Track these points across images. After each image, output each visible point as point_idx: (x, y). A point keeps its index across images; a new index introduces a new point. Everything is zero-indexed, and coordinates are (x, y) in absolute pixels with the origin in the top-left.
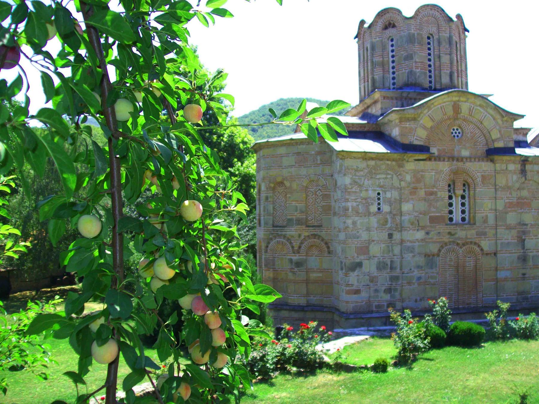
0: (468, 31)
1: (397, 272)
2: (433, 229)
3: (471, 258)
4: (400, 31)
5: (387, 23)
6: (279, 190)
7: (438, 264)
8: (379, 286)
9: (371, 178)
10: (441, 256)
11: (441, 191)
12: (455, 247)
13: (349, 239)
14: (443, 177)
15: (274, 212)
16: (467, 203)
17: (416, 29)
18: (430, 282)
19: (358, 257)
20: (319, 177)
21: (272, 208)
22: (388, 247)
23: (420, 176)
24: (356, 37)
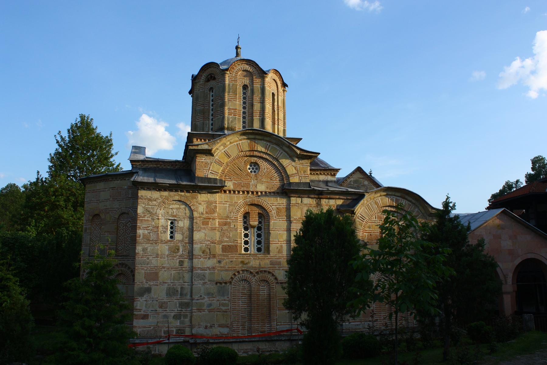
0: (287, 86)
1: (187, 299)
2: (225, 258)
3: (265, 287)
4: (219, 82)
5: (209, 77)
6: (96, 222)
7: (230, 291)
8: (168, 311)
9: (165, 207)
10: (233, 284)
11: (234, 222)
12: (248, 276)
13: (139, 264)
14: (237, 209)
15: (91, 242)
16: (263, 234)
18: (221, 309)
19: (147, 283)
20: (129, 209)
21: (89, 239)
22: (179, 273)
23: (213, 208)
24: (190, 92)
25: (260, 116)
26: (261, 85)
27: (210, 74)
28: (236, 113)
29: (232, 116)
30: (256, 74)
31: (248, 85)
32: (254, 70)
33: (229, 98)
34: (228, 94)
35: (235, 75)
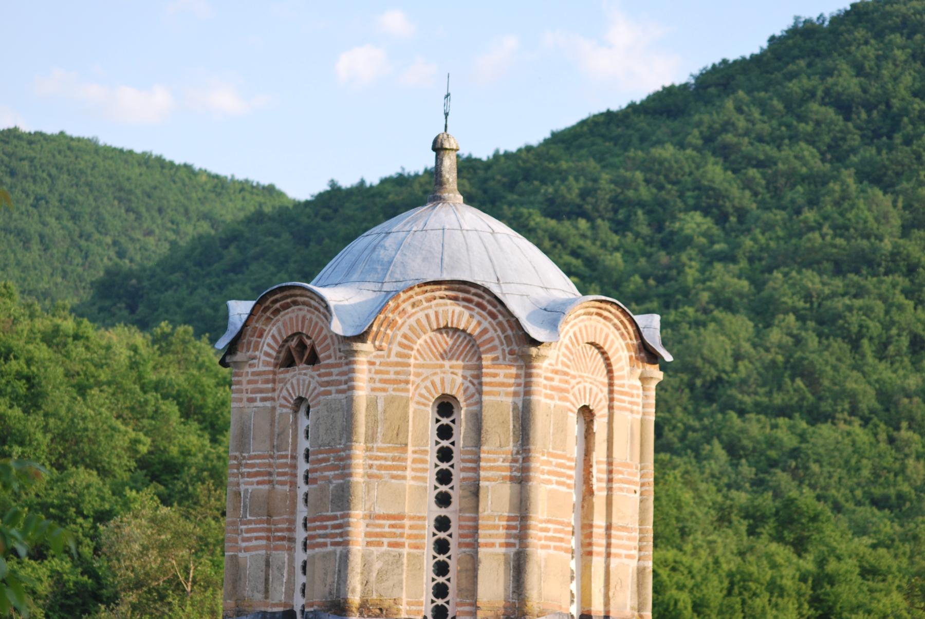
4: (328, 383)
5: (293, 343)
17: (381, 381)
25: (508, 545)
26: (515, 394)
27: (294, 335)
28: (402, 535)
29: (385, 548)
30: (497, 342)
31: (461, 398)
32: (485, 324)
33: (371, 466)
34: (368, 449)
35: (399, 355)
